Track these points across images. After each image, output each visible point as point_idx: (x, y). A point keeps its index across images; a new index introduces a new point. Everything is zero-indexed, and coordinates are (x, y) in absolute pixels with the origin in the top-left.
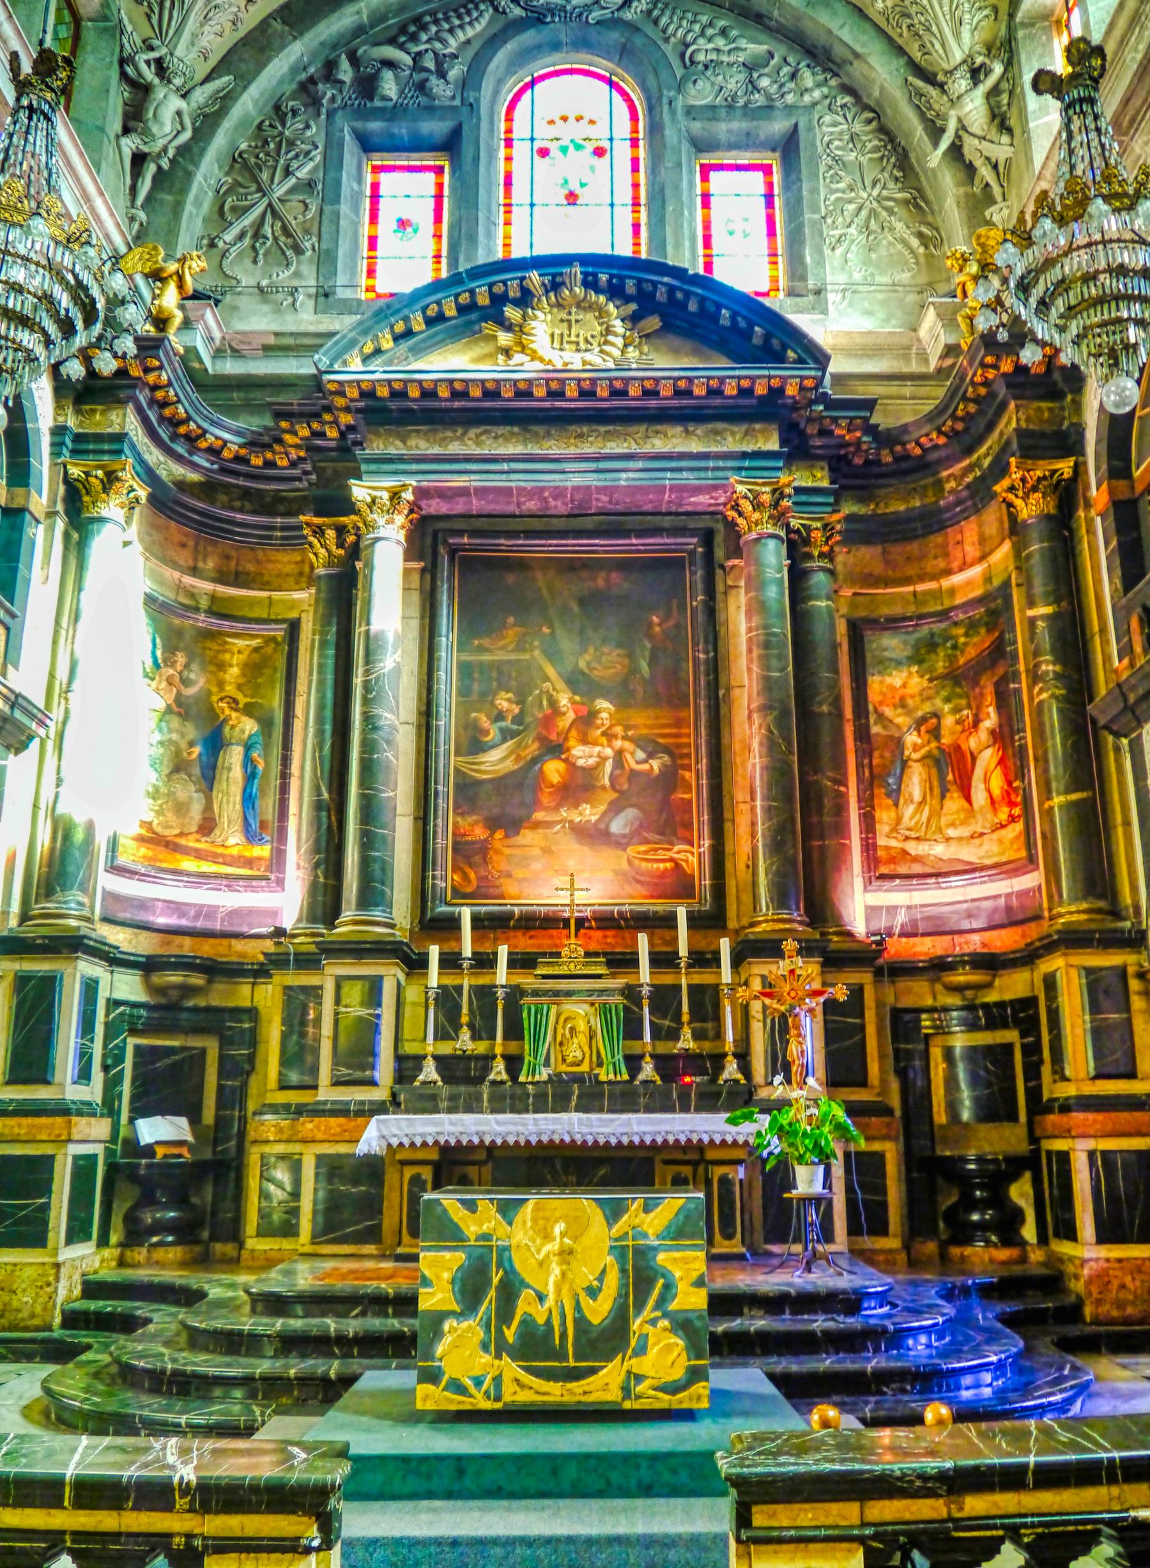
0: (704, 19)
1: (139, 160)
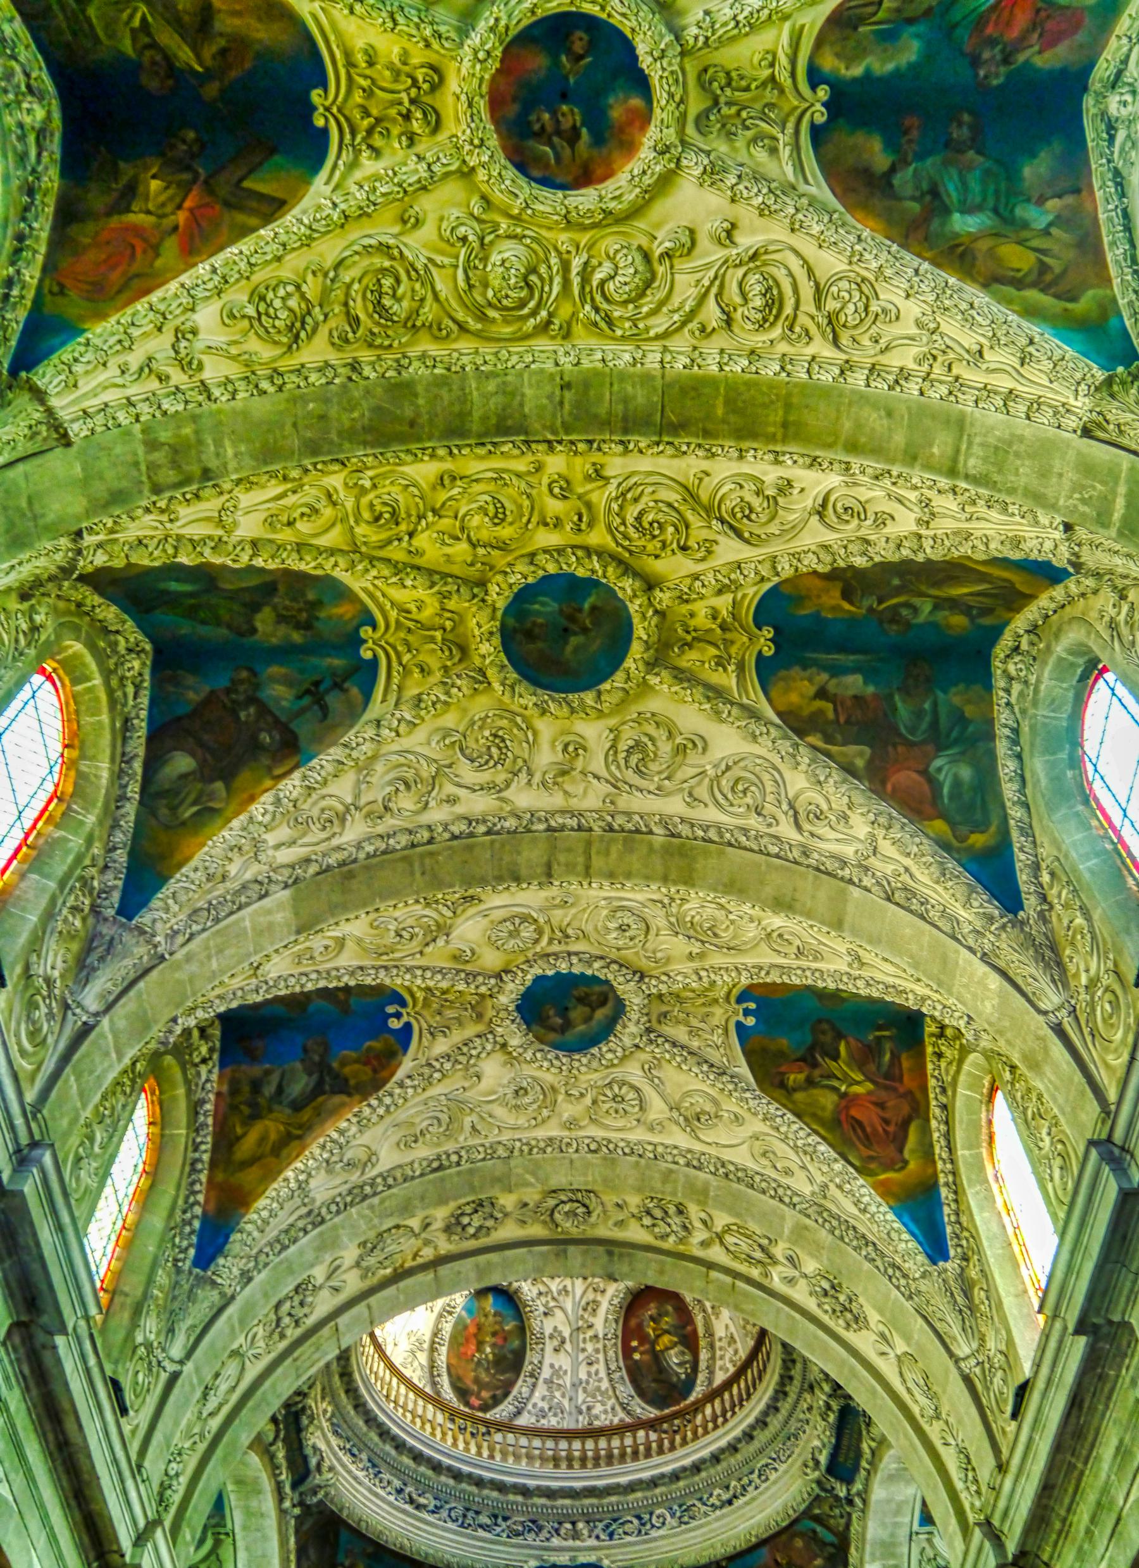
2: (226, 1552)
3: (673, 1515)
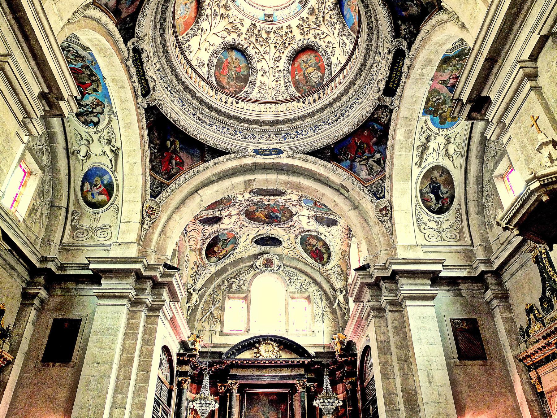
0: (292, 272)
1: (189, 307)
2: (114, 123)
3: (312, 130)
